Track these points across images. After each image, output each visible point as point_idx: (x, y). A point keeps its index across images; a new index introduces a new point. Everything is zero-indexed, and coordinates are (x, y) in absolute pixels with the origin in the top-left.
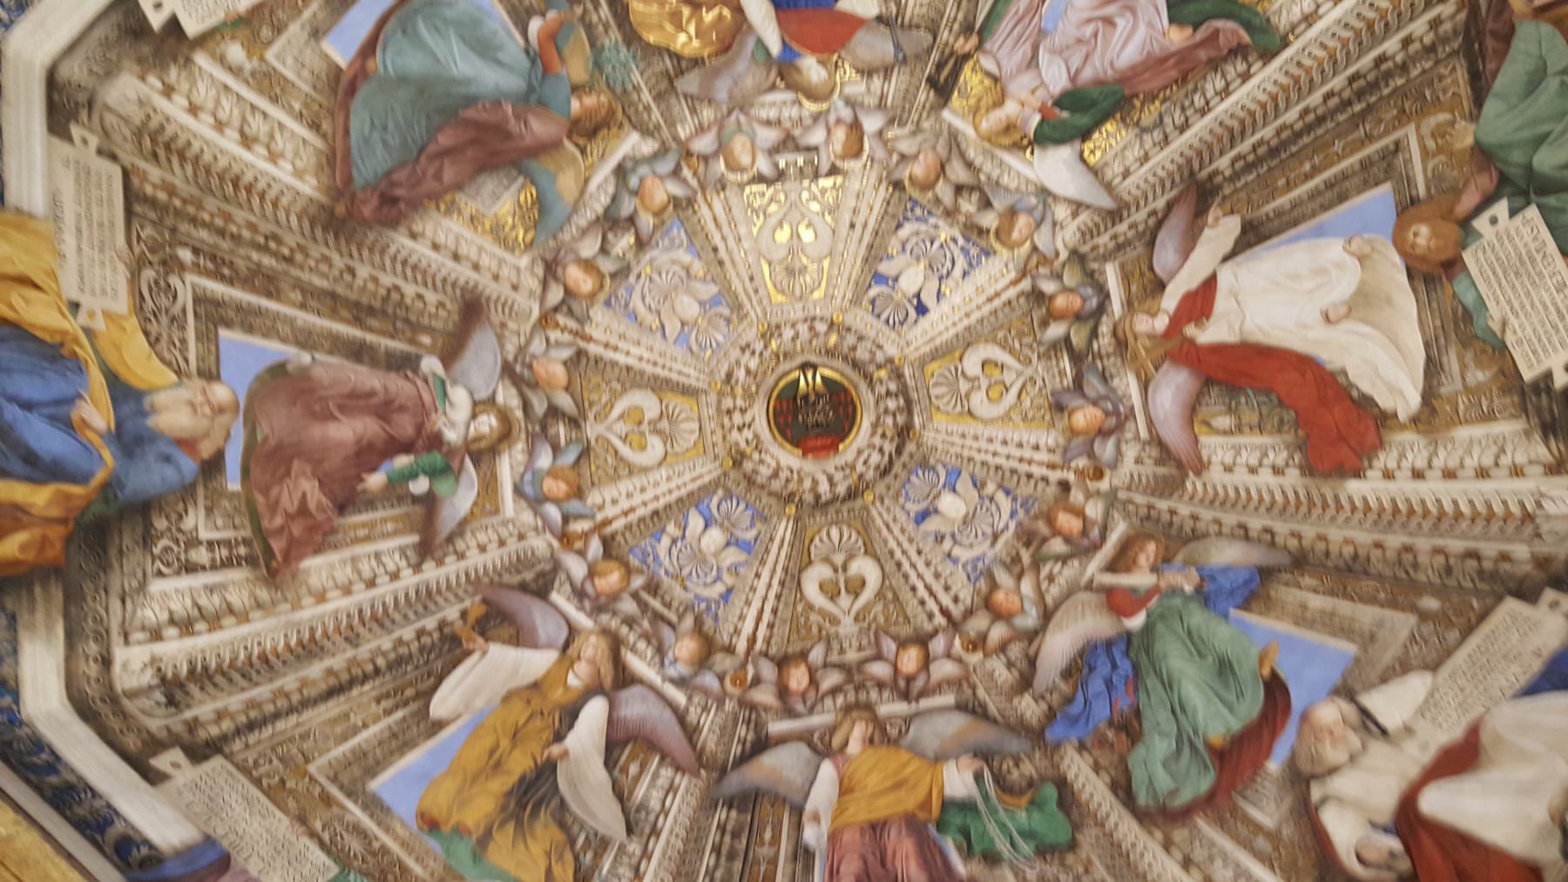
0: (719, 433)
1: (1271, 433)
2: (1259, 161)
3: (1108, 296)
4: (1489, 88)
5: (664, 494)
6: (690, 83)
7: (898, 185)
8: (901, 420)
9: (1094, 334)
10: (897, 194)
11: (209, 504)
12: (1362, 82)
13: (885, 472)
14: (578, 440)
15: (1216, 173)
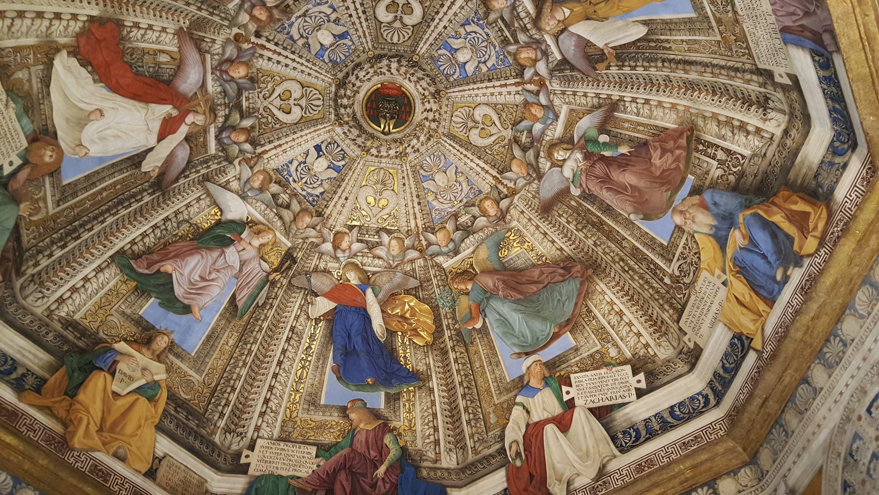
0: (442, 112)
1: (138, 49)
2: (128, 199)
3: (216, 137)
4: (12, 233)
5: (482, 88)
6: (413, 283)
7: (320, 214)
8: (342, 92)
9: (227, 117)
10: (320, 210)
11: (706, 176)
12: (74, 236)
13: (358, 65)
14: (517, 131)
15: (151, 194)
